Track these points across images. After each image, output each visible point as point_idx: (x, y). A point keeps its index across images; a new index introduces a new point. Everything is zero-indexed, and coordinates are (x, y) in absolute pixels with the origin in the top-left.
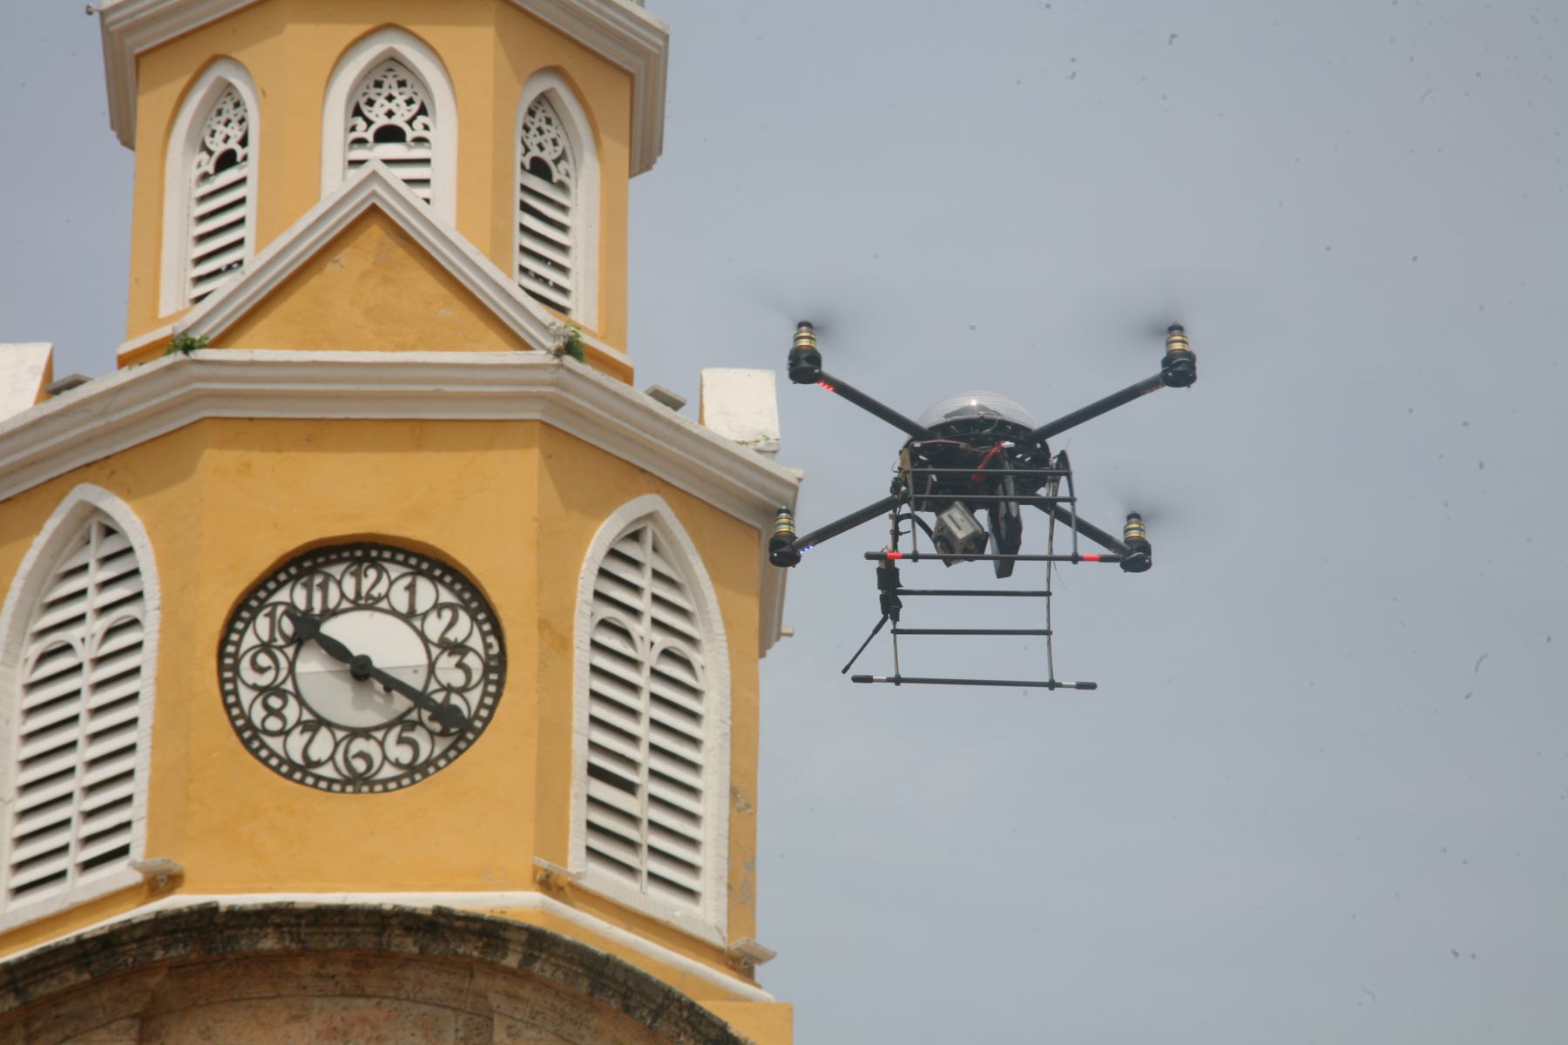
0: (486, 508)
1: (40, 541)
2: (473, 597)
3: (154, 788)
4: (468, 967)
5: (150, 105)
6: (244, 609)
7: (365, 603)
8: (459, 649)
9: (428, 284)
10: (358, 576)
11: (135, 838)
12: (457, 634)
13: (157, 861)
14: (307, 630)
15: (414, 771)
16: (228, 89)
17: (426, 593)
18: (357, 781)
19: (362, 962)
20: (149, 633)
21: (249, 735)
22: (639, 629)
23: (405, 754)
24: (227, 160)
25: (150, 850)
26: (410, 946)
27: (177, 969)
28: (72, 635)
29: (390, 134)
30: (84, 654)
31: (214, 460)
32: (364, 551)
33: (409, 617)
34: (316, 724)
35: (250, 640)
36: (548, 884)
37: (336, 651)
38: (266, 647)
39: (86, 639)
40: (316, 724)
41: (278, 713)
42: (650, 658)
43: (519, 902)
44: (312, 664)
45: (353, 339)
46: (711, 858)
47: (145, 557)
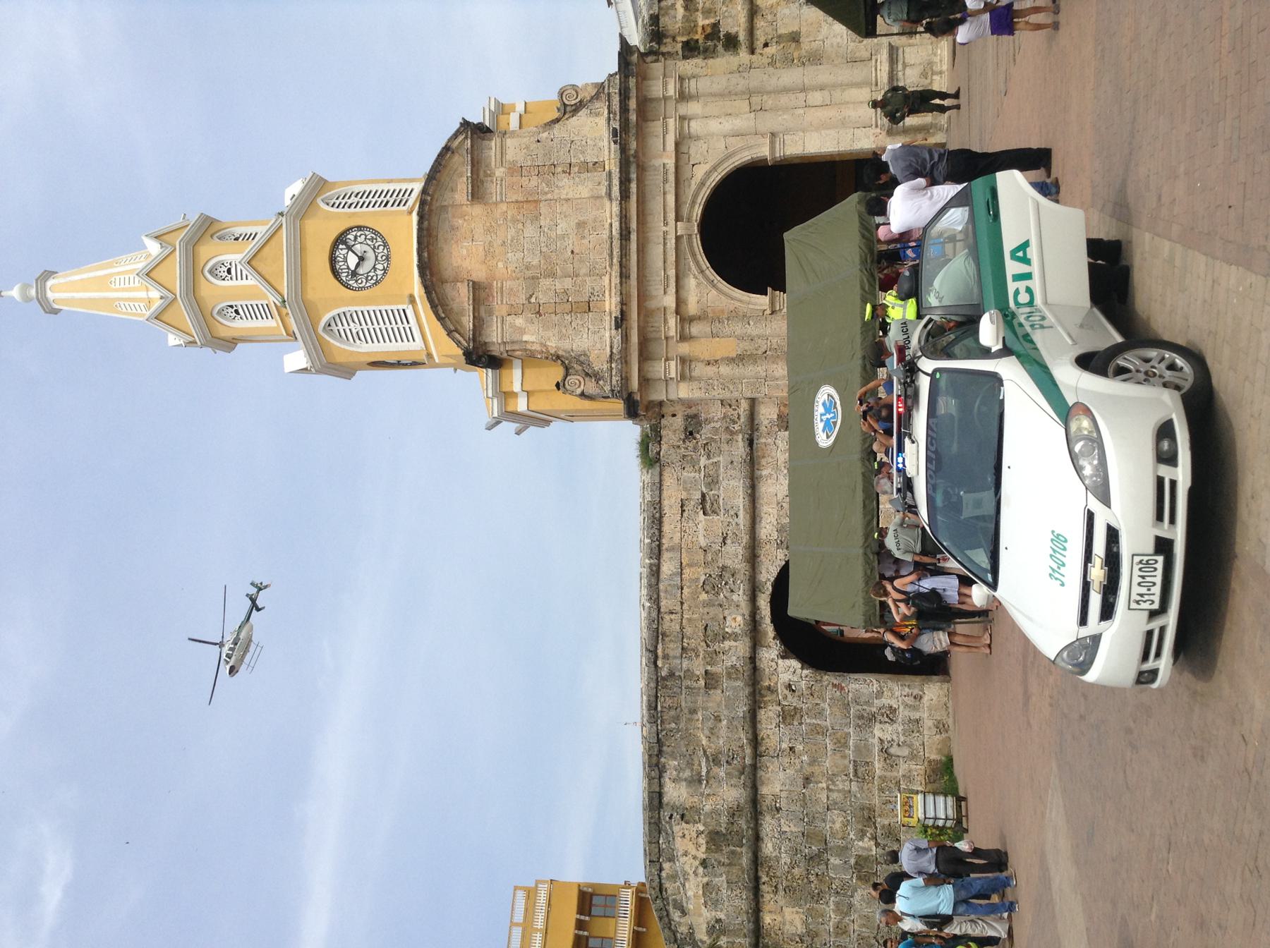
0: (322, 231)
1: (332, 341)
3: (390, 304)
4: (430, 210)
5: (224, 333)
6: (347, 286)
7: (345, 260)
8: (356, 237)
9: (266, 249)
11: (401, 307)
13: (407, 300)
14: (354, 274)
15: (385, 245)
16: (219, 313)
18: (388, 258)
19: (430, 235)
20: (353, 309)
21: (377, 282)
22: (350, 202)
24: (237, 312)
25: (403, 303)
26: (426, 223)
27: (432, 275)
28: (354, 332)
29: (229, 271)
30: (359, 328)
31: (311, 295)
32: (333, 260)
34: (374, 268)
36: (410, 213)
37: (358, 265)
40: (374, 268)
42: (356, 200)
43: (415, 215)
44: (361, 271)
45: (280, 262)
46: (404, 186)
47: (334, 312)
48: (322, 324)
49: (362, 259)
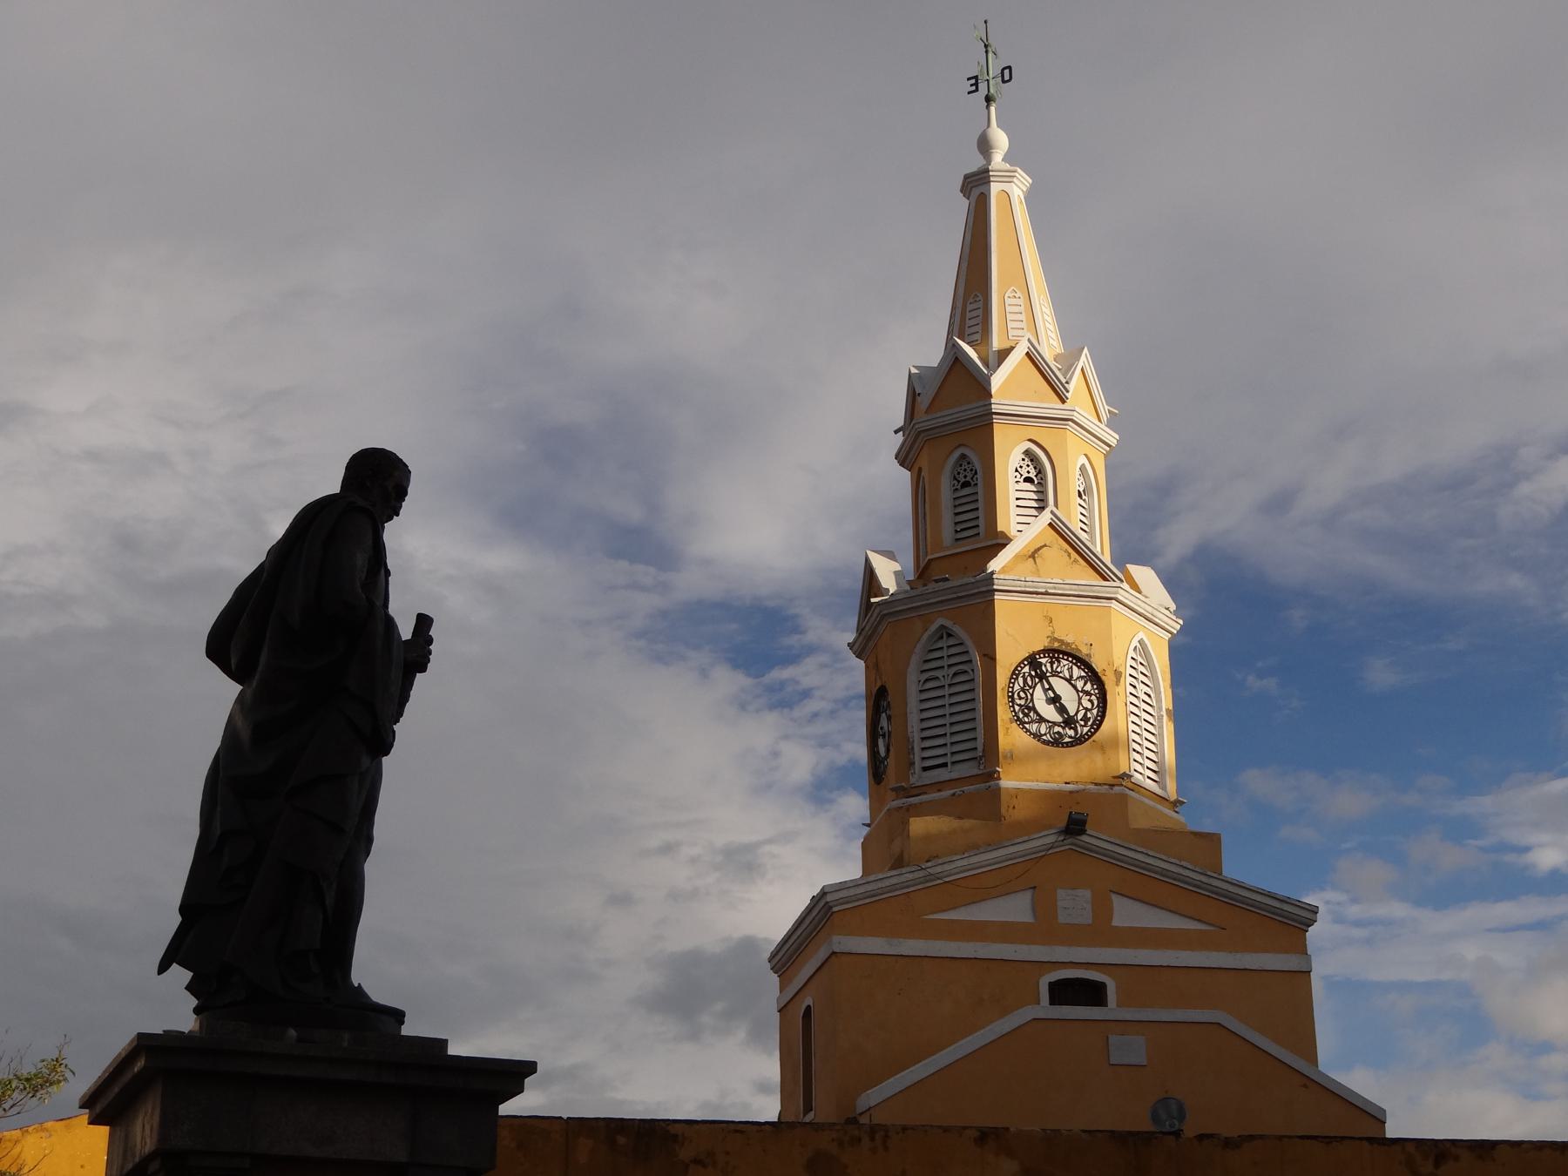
2: (1094, 677)
7: (1055, 674)
8: (1088, 693)
10: (1052, 663)
12: (1088, 687)
16: (963, 456)
17: (1076, 672)
23: (1071, 732)
24: (966, 485)
28: (938, 673)
33: (1069, 681)
34: (1041, 720)
35: (1017, 687)
38: (1023, 690)
39: (944, 676)
41: (1026, 715)
48: (957, 629)
49: (1055, 700)
